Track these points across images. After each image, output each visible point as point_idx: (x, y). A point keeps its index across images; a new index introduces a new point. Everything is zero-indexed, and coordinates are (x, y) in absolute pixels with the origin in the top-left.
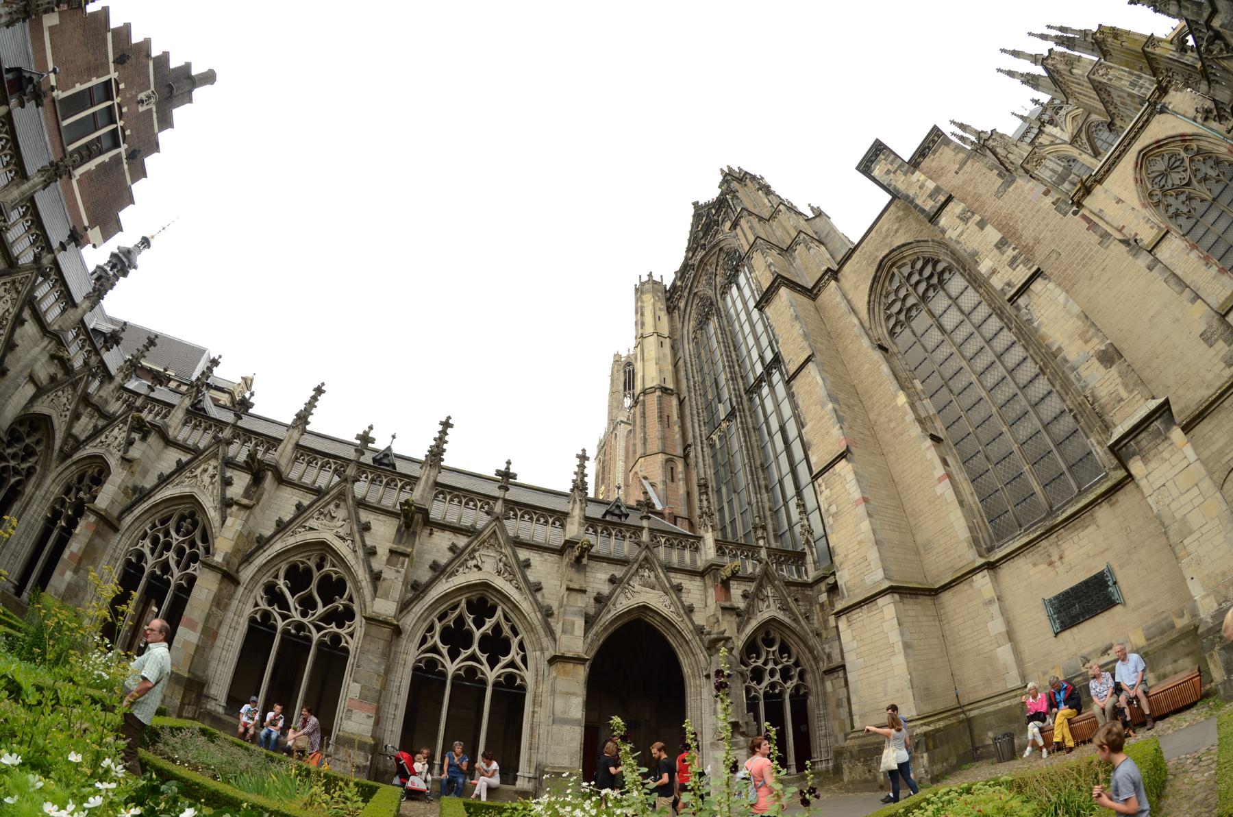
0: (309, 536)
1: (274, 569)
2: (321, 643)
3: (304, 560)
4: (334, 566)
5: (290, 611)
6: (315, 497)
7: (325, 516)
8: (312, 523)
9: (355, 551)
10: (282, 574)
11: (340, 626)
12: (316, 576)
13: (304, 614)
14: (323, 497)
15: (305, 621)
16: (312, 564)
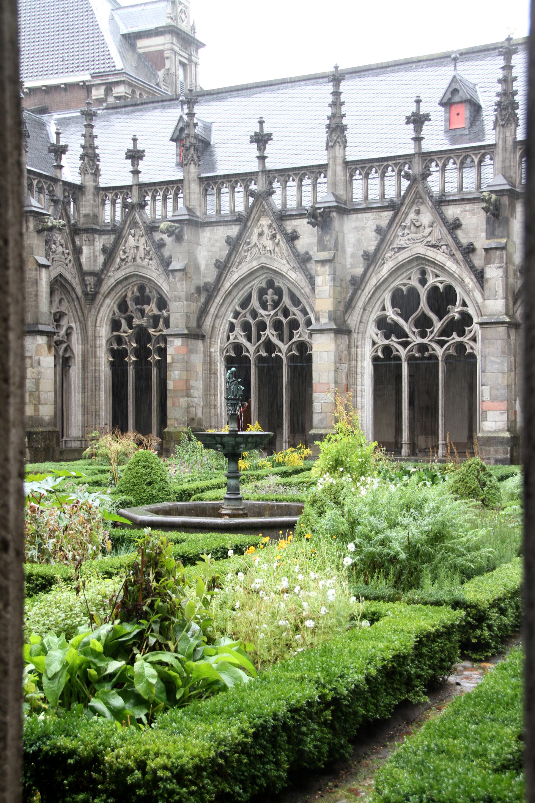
0: (403, 256)
1: (379, 303)
2: (448, 358)
3: (405, 281)
4: (437, 276)
5: (407, 337)
6: (391, 213)
7: (410, 229)
8: (400, 242)
9: (453, 255)
10: (388, 304)
11: (461, 333)
12: (423, 292)
13: (423, 335)
14: (399, 210)
15: (425, 341)
16: (414, 282)
